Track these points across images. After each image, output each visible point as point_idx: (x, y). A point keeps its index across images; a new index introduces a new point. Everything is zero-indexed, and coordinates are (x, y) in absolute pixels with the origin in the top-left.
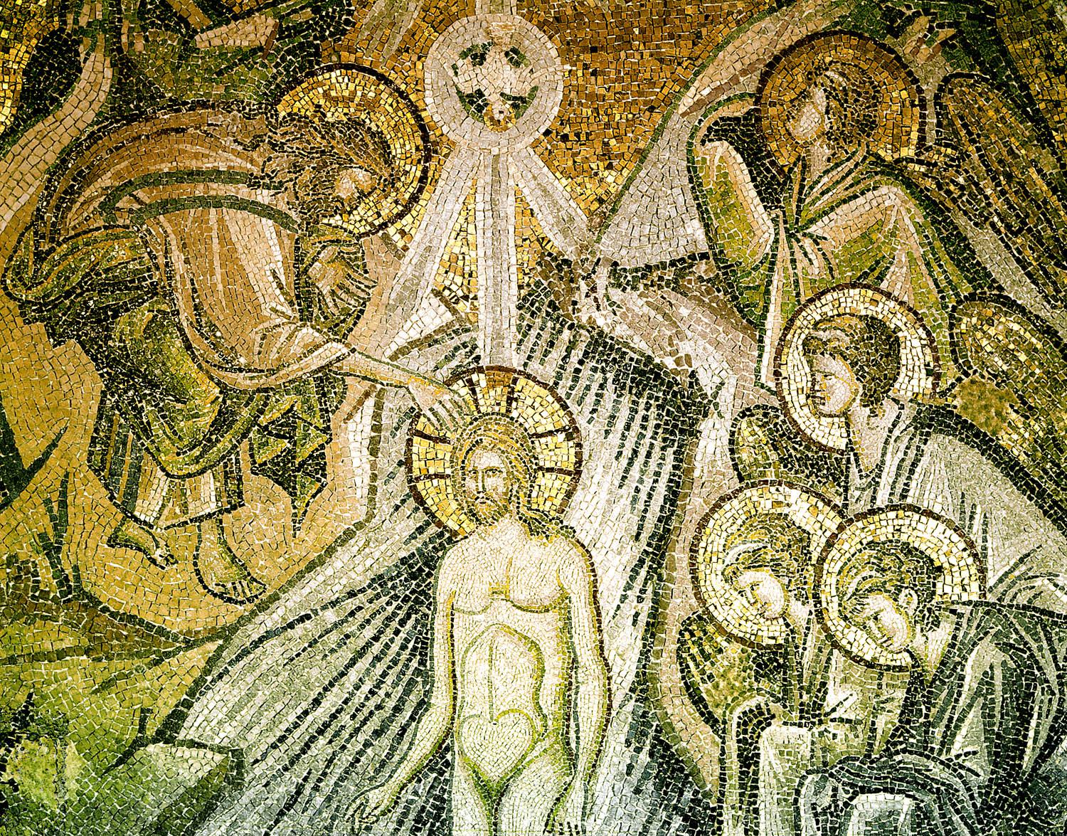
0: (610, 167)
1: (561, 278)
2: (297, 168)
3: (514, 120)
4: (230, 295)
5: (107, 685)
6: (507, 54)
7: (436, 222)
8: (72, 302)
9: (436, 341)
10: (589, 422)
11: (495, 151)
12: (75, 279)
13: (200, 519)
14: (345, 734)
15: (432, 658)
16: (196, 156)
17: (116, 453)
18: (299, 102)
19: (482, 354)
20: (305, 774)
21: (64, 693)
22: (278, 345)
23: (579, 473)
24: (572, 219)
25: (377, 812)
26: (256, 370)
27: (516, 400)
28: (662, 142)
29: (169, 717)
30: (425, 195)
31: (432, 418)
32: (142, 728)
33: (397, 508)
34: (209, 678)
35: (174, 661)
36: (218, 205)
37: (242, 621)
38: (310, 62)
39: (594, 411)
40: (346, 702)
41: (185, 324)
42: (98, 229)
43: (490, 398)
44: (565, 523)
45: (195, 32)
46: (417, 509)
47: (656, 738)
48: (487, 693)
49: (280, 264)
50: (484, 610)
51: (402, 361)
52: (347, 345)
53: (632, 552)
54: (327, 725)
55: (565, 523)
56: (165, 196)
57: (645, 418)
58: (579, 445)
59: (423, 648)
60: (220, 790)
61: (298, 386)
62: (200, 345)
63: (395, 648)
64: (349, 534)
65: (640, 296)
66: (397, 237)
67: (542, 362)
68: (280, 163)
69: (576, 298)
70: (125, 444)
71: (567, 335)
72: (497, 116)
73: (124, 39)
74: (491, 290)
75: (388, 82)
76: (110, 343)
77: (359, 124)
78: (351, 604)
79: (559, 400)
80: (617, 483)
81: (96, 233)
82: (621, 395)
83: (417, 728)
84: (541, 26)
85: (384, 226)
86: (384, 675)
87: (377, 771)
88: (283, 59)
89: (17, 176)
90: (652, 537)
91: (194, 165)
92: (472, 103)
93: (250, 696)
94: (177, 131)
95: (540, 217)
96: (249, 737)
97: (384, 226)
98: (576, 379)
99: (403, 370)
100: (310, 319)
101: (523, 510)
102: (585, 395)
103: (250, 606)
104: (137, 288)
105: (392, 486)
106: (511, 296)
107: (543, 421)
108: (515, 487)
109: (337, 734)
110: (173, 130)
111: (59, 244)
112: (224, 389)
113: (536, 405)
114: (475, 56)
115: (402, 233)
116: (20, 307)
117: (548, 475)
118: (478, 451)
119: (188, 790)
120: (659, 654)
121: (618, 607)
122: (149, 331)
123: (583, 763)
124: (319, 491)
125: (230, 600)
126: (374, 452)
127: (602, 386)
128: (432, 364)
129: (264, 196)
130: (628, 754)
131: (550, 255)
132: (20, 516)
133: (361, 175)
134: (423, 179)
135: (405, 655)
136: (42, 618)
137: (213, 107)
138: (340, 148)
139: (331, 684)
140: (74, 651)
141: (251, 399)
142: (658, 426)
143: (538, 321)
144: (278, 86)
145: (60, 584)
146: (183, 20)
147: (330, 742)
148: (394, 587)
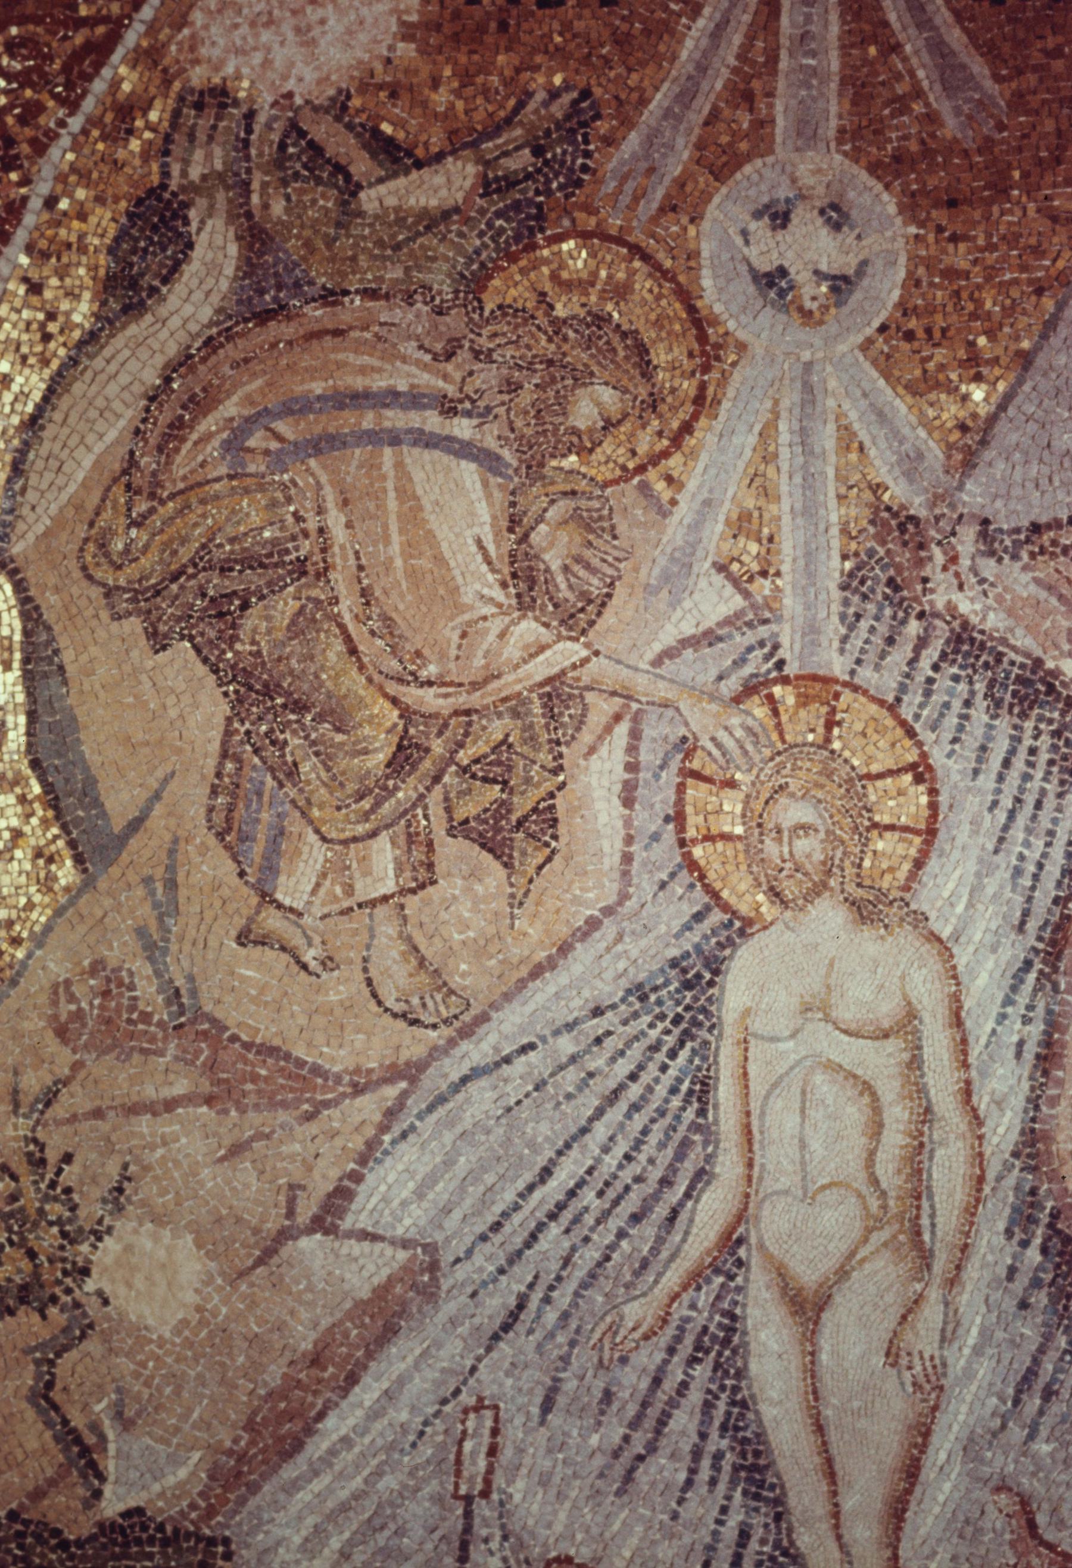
0: (978, 378)
1: (905, 544)
2: (512, 387)
3: (833, 311)
4: (412, 574)
5: (236, 1150)
6: (822, 212)
7: (716, 464)
8: (182, 587)
9: (720, 639)
10: (949, 756)
11: (806, 356)
12: (185, 554)
13: (373, 903)
14: (589, 1220)
15: (716, 1107)
16: (363, 370)
17: (248, 807)
18: (510, 288)
19: (787, 656)
20: (529, 1278)
21: (177, 1163)
22: (485, 646)
23: (931, 832)
24: (920, 456)
25: (637, 1335)
26: (451, 684)
27: (839, 724)
28: (1055, 341)
29: (329, 1196)
30: (703, 422)
31: (715, 752)
32: (291, 1213)
33: (663, 885)
34: (387, 1138)
35: (334, 1113)
36: (395, 440)
37: (435, 1053)
38: (531, 230)
39: (955, 740)
40: (590, 1171)
41: (347, 618)
42: (218, 480)
43: (804, 725)
44: (913, 906)
45: (359, 187)
46: (692, 886)
47: (1051, 1226)
48: (797, 1157)
49: (487, 528)
50: (793, 1036)
51: (669, 667)
52: (587, 645)
53: (1013, 950)
54: (561, 1207)
55: (913, 906)
56: (318, 430)
57: (1033, 751)
58: (933, 792)
59: (702, 1091)
60: (404, 1304)
61: (515, 706)
62: (371, 648)
63: (661, 1090)
64: (593, 924)
65: (1025, 568)
66: (660, 486)
67: (877, 667)
68: (487, 377)
69: (927, 572)
70: (259, 794)
71: (914, 627)
72: (808, 304)
73: (255, 199)
74: (801, 562)
75: (646, 258)
76: (238, 646)
77: (600, 320)
78: (595, 1026)
79: (903, 723)
80: (990, 847)
81: (217, 486)
82: (994, 717)
83: (694, 1211)
84: (874, 169)
85: (641, 469)
86: (645, 1132)
87: (637, 1274)
88: (490, 225)
89: (100, 402)
90: (1042, 928)
91: (359, 383)
92: (771, 285)
93: (449, 1163)
94: (338, 333)
95: (873, 452)
96: (447, 1224)
97: (641, 469)
98: (928, 694)
99: (672, 681)
100: (532, 608)
101: (850, 888)
102: (942, 715)
103: (446, 1032)
104: (276, 565)
105: (658, 851)
106: (834, 568)
107: (880, 756)
108: (839, 854)
109: (577, 1220)
110: (327, 332)
111: (163, 502)
112: (406, 713)
113: (869, 731)
114: (774, 217)
115: (669, 479)
116: (107, 595)
117: (888, 835)
118: (783, 800)
119: (361, 1306)
120: (1054, 1101)
121: (994, 1032)
122: (295, 630)
123: (941, 1264)
124: (549, 859)
125: (415, 1022)
126: (628, 802)
127: (967, 704)
128: (713, 673)
129: (463, 428)
130: (1009, 1250)
131: (888, 509)
132: (107, 902)
133: (607, 395)
134: (699, 400)
135: (676, 1102)
136: (143, 1051)
137: (387, 297)
138: (579, 356)
139: (568, 1146)
140: (188, 1100)
141: (445, 725)
142: (1051, 763)
143: (871, 608)
144: (483, 265)
145: (168, 1003)
146: (339, 169)
147: (567, 1231)
148: (659, 1002)
